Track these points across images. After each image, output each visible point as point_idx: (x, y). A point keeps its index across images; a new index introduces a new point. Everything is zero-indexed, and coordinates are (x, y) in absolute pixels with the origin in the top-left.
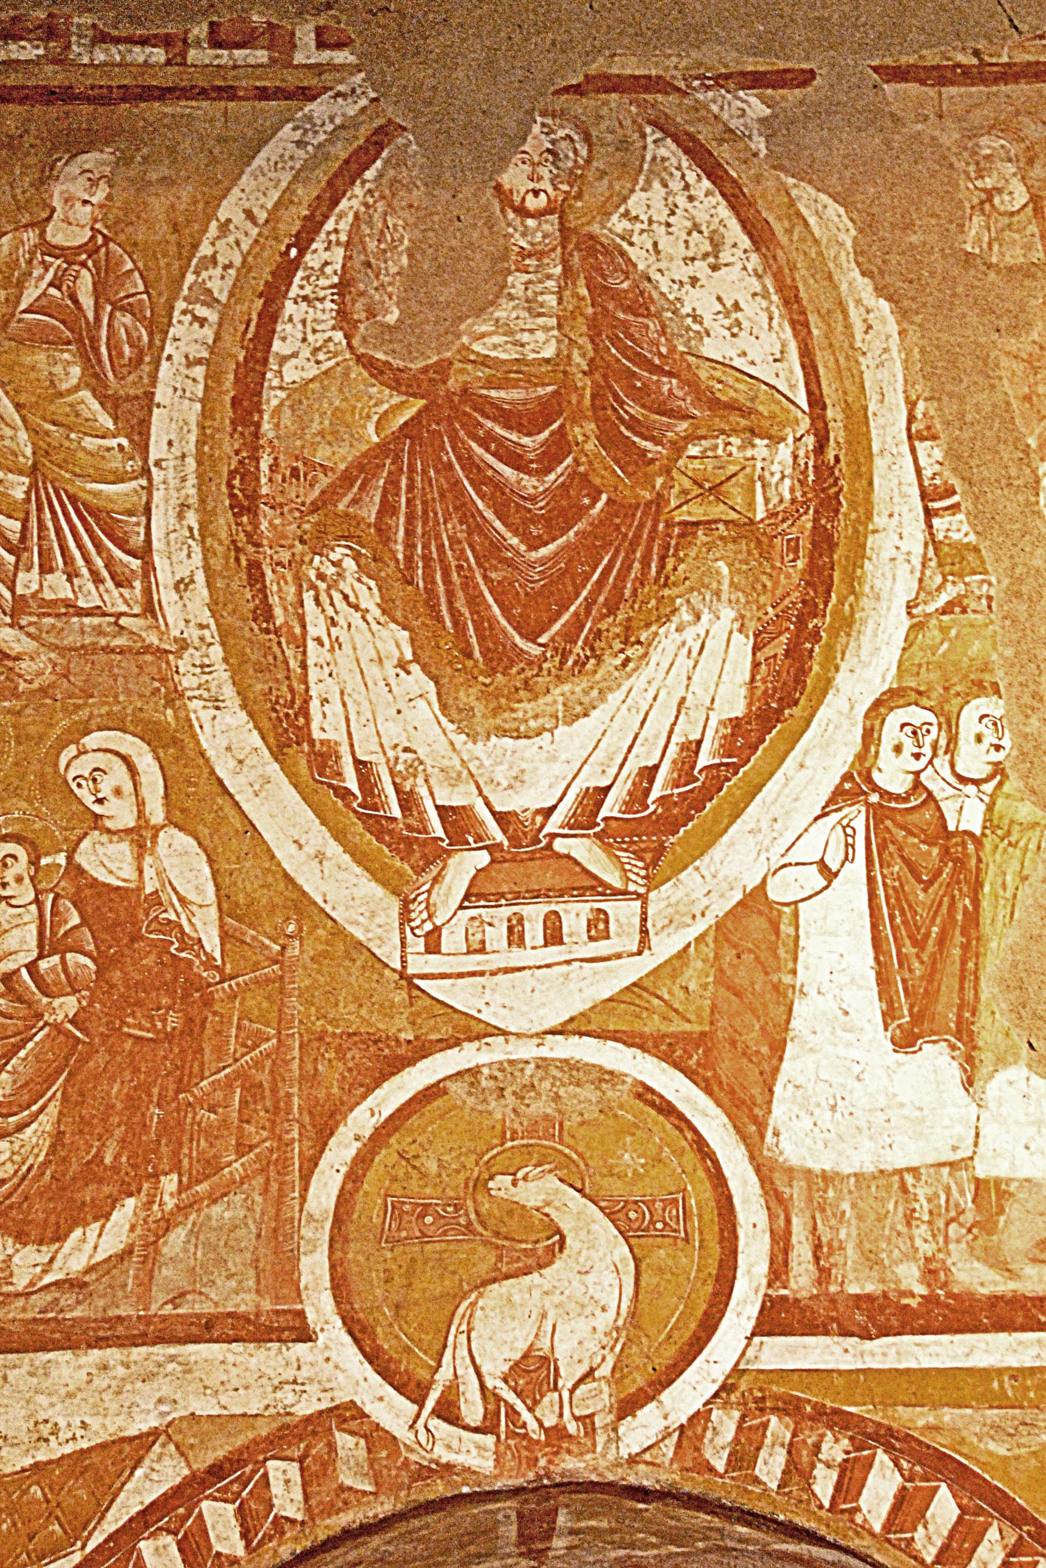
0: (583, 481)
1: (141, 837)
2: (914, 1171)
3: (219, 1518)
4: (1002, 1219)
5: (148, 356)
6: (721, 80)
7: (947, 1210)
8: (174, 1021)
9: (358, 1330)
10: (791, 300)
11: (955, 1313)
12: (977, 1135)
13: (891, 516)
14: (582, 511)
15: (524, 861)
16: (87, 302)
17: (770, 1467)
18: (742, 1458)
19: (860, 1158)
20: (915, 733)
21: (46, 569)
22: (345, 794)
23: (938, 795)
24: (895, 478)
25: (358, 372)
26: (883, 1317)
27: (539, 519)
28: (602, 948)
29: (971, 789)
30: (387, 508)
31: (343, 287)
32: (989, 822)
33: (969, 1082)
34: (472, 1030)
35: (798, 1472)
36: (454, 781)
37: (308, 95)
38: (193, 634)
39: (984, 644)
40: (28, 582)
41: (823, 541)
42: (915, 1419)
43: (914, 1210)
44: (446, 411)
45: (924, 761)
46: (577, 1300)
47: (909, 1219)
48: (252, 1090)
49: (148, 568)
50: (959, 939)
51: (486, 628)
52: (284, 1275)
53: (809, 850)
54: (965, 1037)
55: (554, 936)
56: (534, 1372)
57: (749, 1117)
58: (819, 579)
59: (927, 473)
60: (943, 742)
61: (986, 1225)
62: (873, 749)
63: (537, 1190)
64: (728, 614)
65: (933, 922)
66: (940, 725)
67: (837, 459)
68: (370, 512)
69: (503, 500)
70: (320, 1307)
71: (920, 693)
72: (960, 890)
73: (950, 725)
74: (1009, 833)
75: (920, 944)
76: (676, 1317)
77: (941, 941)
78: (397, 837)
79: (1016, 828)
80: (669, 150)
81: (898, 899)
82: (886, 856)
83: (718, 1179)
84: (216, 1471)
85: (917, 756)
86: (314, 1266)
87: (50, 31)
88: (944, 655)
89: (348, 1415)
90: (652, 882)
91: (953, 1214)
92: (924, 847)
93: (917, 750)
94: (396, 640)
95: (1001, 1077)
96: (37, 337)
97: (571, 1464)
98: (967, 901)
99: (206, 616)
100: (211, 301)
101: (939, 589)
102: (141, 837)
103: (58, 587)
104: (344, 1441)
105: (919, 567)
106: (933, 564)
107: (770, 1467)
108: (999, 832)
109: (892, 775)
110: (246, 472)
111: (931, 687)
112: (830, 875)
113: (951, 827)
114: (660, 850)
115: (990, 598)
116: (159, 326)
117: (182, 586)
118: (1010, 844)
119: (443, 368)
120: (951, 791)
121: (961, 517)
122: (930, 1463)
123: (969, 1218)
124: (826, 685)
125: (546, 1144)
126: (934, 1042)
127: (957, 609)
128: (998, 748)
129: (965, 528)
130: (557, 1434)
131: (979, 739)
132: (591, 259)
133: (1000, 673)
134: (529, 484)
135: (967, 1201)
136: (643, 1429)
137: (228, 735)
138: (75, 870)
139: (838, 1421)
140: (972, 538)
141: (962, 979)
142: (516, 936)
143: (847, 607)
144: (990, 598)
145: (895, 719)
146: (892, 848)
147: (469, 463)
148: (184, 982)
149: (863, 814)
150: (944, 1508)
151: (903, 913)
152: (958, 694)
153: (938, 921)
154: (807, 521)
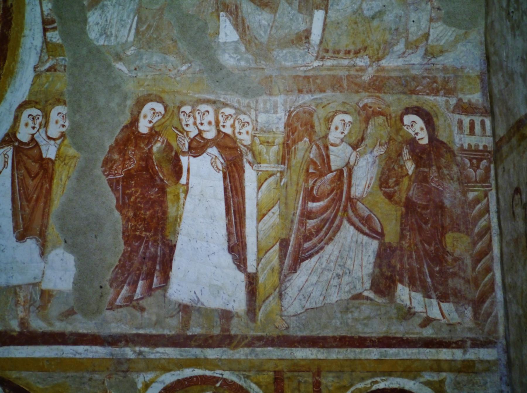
2: (20, 286)
4: (49, 305)
7: (30, 301)
11: (29, 338)
12: (43, 274)
13: (30, 30)
20: (33, 119)
23: (41, 144)
29: (52, 142)
32: (58, 156)
33: (42, 254)
39: (61, 83)
43: (18, 301)
45: (36, 130)
47: (17, 304)
50: (43, 200)
59: (46, 13)
60: (43, 123)
61: (43, 307)
62: (17, 124)
65: (34, 193)
66: (43, 116)
67: (12, 5)
71: (36, 103)
72: (45, 181)
73: (46, 116)
74: (65, 160)
75: (29, 201)
77: (37, 200)
79: (67, 158)
81: (22, 183)
82: (19, 167)
85: (34, 128)
88: (47, 88)
91: (32, 302)
92: (33, 164)
93: (33, 125)
95: (54, 253)
98: (47, 185)
101: (47, 61)
105: (39, 52)
106: (45, 51)
108: (61, 159)
109: (24, 135)
111: (40, 101)
113: (44, 156)
115: (65, 66)
118: (65, 164)
120: (45, 142)
121: (57, 32)
123: (38, 304)
126: (31, 238)
127: (53, 70)
128: (63, 126)
129: (58, 37)
131: (57, 122)
133: (67, 96)
135: (38, 298)
140: (60, 41)
141: (43, 215)
143: (12, 66)
144: (65, 66)
145: (26, 113)
146: (22, 164)
149: (12, 150)
151: (24, 189)
152: (50, 104)
153: (36, 193)
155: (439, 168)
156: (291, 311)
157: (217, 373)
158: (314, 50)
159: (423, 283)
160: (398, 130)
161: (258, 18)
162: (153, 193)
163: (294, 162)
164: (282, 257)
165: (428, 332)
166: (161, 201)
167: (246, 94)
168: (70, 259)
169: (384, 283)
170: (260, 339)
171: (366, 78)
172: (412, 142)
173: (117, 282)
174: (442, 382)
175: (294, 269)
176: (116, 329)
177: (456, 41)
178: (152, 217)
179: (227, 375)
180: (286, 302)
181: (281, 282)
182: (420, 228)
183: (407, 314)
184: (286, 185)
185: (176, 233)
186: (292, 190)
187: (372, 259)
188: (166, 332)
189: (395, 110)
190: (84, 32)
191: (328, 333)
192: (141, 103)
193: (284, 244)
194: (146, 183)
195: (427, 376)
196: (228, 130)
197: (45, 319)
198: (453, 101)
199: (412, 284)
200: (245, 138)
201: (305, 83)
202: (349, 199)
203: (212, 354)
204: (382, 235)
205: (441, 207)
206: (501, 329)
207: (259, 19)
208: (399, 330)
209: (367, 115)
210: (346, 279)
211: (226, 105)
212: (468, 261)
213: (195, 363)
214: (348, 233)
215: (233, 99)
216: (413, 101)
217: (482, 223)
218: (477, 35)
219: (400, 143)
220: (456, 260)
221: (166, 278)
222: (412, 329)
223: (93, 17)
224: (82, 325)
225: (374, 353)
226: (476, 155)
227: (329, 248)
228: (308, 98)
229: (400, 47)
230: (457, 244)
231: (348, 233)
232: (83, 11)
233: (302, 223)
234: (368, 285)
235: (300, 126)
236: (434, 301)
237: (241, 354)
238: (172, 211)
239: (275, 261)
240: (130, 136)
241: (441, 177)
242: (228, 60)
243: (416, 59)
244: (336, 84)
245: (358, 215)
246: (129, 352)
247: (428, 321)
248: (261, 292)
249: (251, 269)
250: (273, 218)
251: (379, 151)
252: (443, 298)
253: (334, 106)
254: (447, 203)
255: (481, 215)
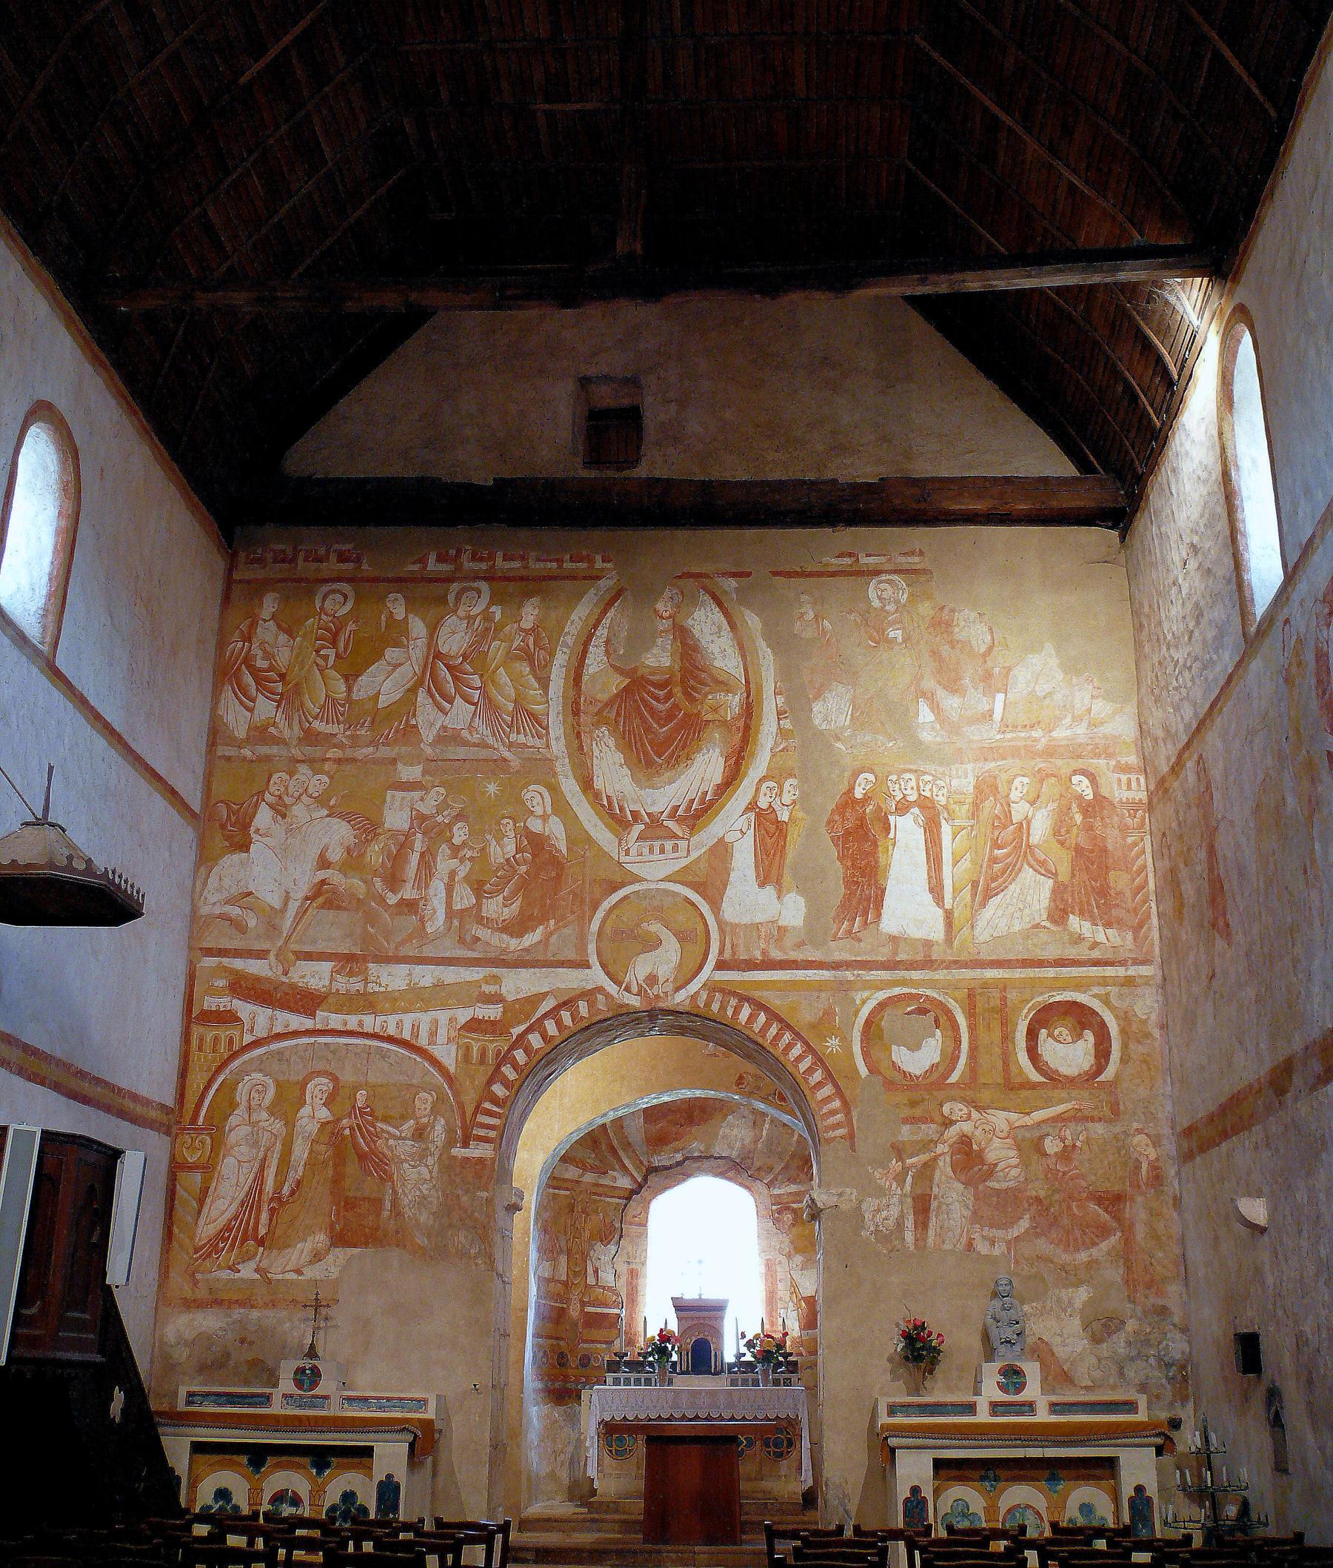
0: (676, 707)
1: (545, 818)
3: (566, 1016)
5: (548, 665)
6: (724, 574)
8: (553, 874)
9: (603, 966)
10: (741, 648)
14: (675, 716)
15: (655, 829)
16: (532, 647)
17: (715, 1007)
18: (708, 1004)
19: (746, 920)
21: (518, 733)
22: (603, 806)
24: (770, 705)
25: (611, 670)
26: (750, 965)
27: (661, 717)
28: (676, 855)
30: (618, 714)
31: (607, 642)
34: (637, 879)
35: (723, 1008)
36: (635, 802)
37: (599, 578)
38: (560, 755)
40: (513, 737)
41: (747, 728)
42: (756, 994)
44: (637, 685)
46: (663, 961)
48: (575, 895)
49: (548, 733)
51: (646, 754)
52: (582, 946)
53: (737, 826)
54: (778, 884)
55: (662, 851)
56: (652, 980)
57: (716, 905)
58: (746, 740)
63: (655, 927)
64: (718, 751)
68: (613, 715)
69: (652, 711)
70: (593, 959)
73: (781, 787)
76: (693, 965)
78: (619, 820)
80: (707, 597)
83: (706, 924)
84: (565, 1003)
86: (592, 948)
87: (523, 558)
89: (600, 990)
90: (691, 835)
94: (619, 757)
96: (518, 658)
97: (661, 1005)
99: (564, 749)
100: (568, 647)
102: (545, 818)
103: (522, 739)
104: (600, 997)
107: (715, 1007)
109: (763, 803)
110: (576, 703)
111: (776, 775)
112: (743, 834)
114: (694, 826)
116: (552, 654)
117: (557, 739)
119: (635, 670)
122: (759, 1006)
124: (745, 774)
125: (659, 913)
130: (657, 996)
132: (683, 635)
134: (661, 707)
136: (681, 996)
137: (570, 786)
138: (526, 827)
139: (734, 994)
142: (651, 851)
147: (643, 700)
148: (556, 863)
150: (762, 1018)
154: (741, 723)
155: (1102, 819)
156: (981, 939)
157: (921, 991)
158: (996, 726)
159: (1091, 912)
160: (1068, 788)
161: (950, 702)
162: (867, 847)
163: (981, 817)
164: (974, 895)
165: (1096, 954)
166: (874, 853)
167: (941, 764)
168: (801, 901)
169: (1059, 914)
170: (956, 962)
171: (1040, 746)
172: (1080, 798)
173: (839, 919)
174: (1107, 994)
175: (983, 904)
176: (838, 956)
177: (1114, 713)
178: (867, 865)
179: (929, 992)
180: (976, 932)
181: (973, 916)
182: (1087, 868)
183: (1078, 939)
184: (976, 836)
185: (886, 878)
186: (981, 840)
187: (1048, 895)
188: (880, 958)
189: (1065, 771)
190: (809, 719)
191: (1011, 956)
192: (856, 774)
193: (975, 884)
194: (860, 838)
195: (1096, 990)
196: (927, 794)
197: (782, 949)
198: (1113, 763)
199: (1082, 914)
200: (943, 800)
201: (989, 752)
202: (1028, 846)
203: (916, 975)
204: (1056, 874)
205: (1105, 850)
206: (1157, 950)
207: (951, 703)
208: (1072, 953)
209: (1041, 777)
210: (1027, 911)
211: (926, 773)
212: (1128, 894)
213: (903, 983)
214: (1028, 874)
215: (930, 767)
216: (1080, 764)
217: (1139, 862)
218: (1131, 709)
219: (1068, 800)
220: (1117, 894)
221: (879, 915)
222: (1081, 952)
223: (817, 707)
224: (811, 954)
225: (1051, 972)
226: (1133, 807)
227: (1012, 887)
228: (993, 764)
229: (1068, 720)
230: (1119, 881)
231: (1028, 874)
232: (809, 702)
233: (990, 867)
234: (1045, 916)
235: (987, 788)
236: (1100, 928)
237: (940, 975)
238: (882, 860)
239: (968, 898)
240: (848, 802)
241: (1104, 825)
242: (926, 736)
243: (1081, 730)
244: (1015, 752)
245: (1036, 860)
246: (849, 975)
247: (1095, 945)
248: (956, 923)
249: (948, 902)
250: (965, 864)
251: (1052, 806)
252: (1108, 925)
253: (1015, 771)
254: (1110, 847)
255: (1138, 857)
